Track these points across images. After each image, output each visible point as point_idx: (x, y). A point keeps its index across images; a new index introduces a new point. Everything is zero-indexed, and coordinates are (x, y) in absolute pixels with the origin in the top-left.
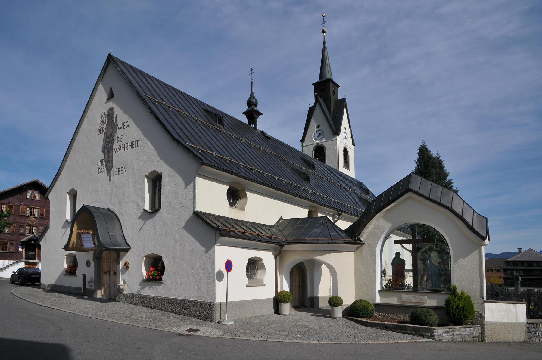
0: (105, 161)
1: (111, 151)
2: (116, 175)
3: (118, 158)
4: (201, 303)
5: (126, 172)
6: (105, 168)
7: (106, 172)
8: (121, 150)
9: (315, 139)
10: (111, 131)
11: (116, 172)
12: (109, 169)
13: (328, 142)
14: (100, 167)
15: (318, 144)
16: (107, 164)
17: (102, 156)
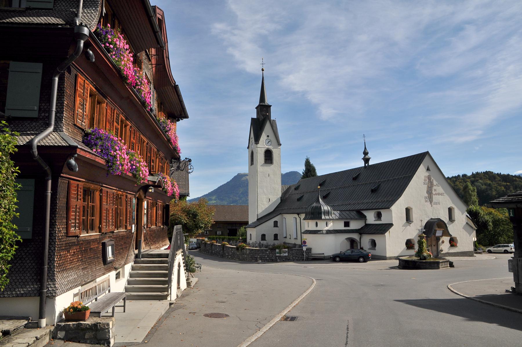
0: (428, 197)
1: (432, 194)
3: (435, 198)
4: (470, 252)
6: (429, 201)
7: (429, 202)
9: (266, 144)
12: (431, 202)
13: (274, 149)
14: (426, 200)
15: (268, 148)
17: (427, 195)
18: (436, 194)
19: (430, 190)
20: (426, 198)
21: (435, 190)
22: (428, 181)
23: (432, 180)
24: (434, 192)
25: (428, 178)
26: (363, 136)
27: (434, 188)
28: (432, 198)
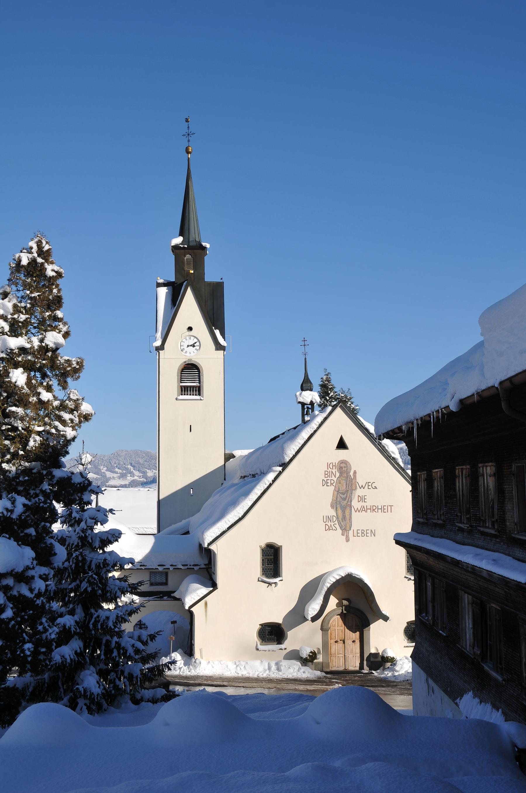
0: (337, 518)
1: (348, 508)
2: (358, 536)
5: (374, 535)
6: (337, 526)
7: (339, 531)
8: (365, 510)
10: (346, 487)
11: (358, 533)
14: (329, 524)
16: (342, 523)
17: (332, 513)
18: (364, 509)
19: (345, 499)
20: (329, 519)
21: (362, 499)
22: (338, 475)
23: (351, 474)
24: (355, 504)
25: (340, 469)
26: (303, 343)
27: (359, 492)
28: (351, 517)
